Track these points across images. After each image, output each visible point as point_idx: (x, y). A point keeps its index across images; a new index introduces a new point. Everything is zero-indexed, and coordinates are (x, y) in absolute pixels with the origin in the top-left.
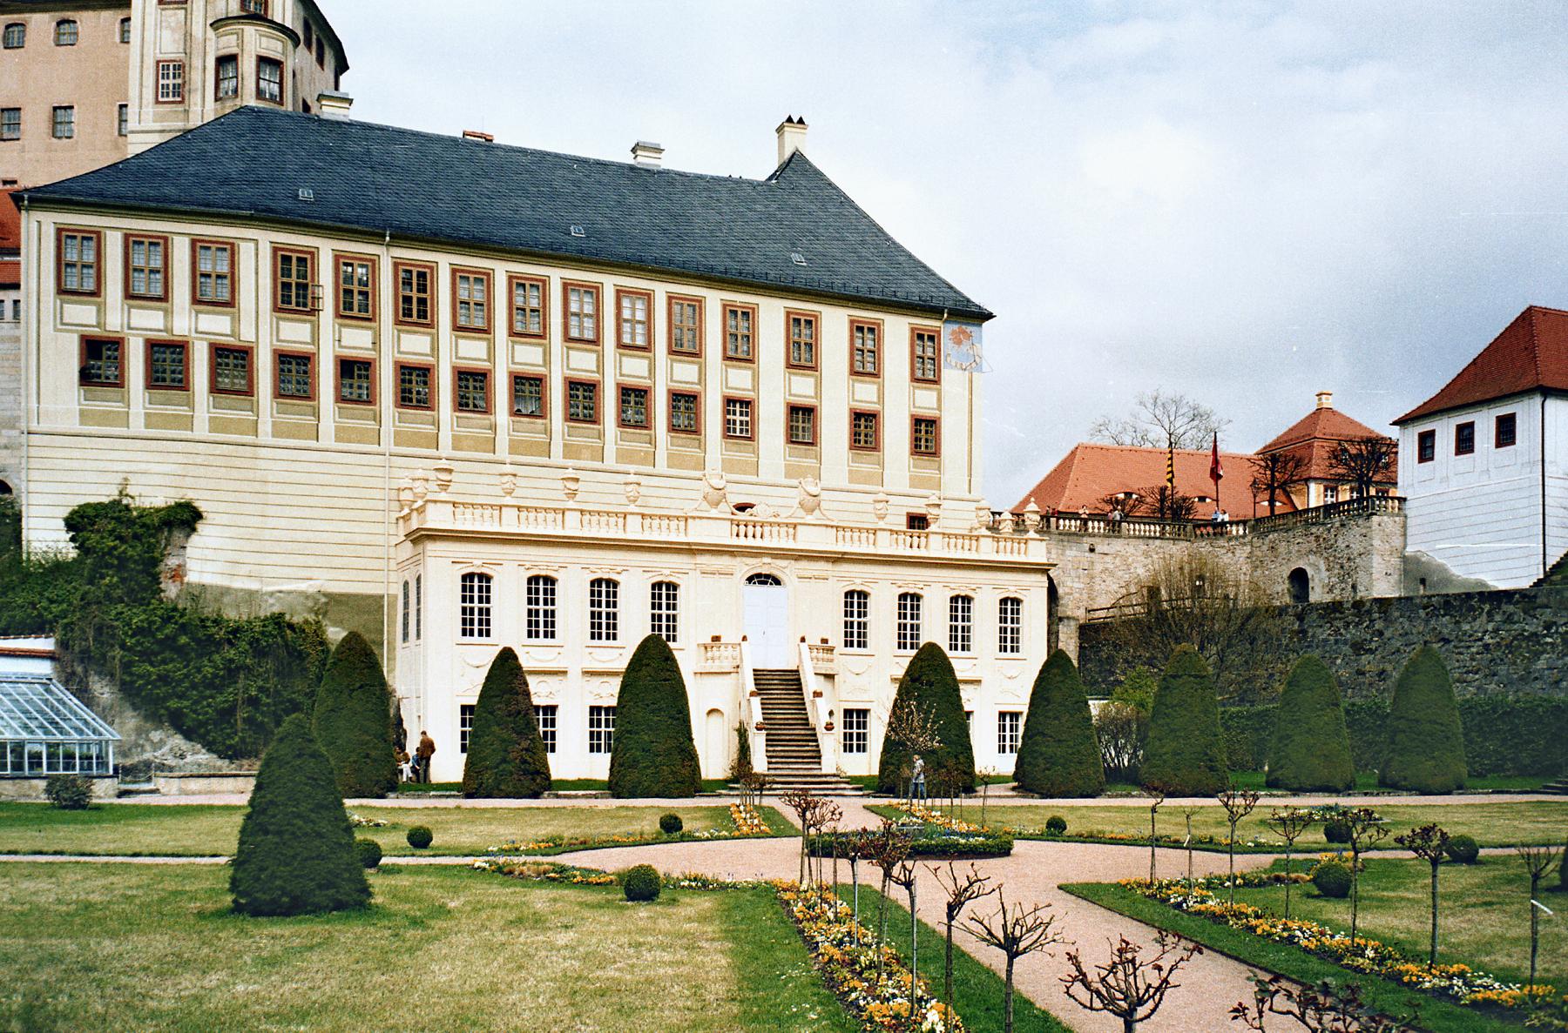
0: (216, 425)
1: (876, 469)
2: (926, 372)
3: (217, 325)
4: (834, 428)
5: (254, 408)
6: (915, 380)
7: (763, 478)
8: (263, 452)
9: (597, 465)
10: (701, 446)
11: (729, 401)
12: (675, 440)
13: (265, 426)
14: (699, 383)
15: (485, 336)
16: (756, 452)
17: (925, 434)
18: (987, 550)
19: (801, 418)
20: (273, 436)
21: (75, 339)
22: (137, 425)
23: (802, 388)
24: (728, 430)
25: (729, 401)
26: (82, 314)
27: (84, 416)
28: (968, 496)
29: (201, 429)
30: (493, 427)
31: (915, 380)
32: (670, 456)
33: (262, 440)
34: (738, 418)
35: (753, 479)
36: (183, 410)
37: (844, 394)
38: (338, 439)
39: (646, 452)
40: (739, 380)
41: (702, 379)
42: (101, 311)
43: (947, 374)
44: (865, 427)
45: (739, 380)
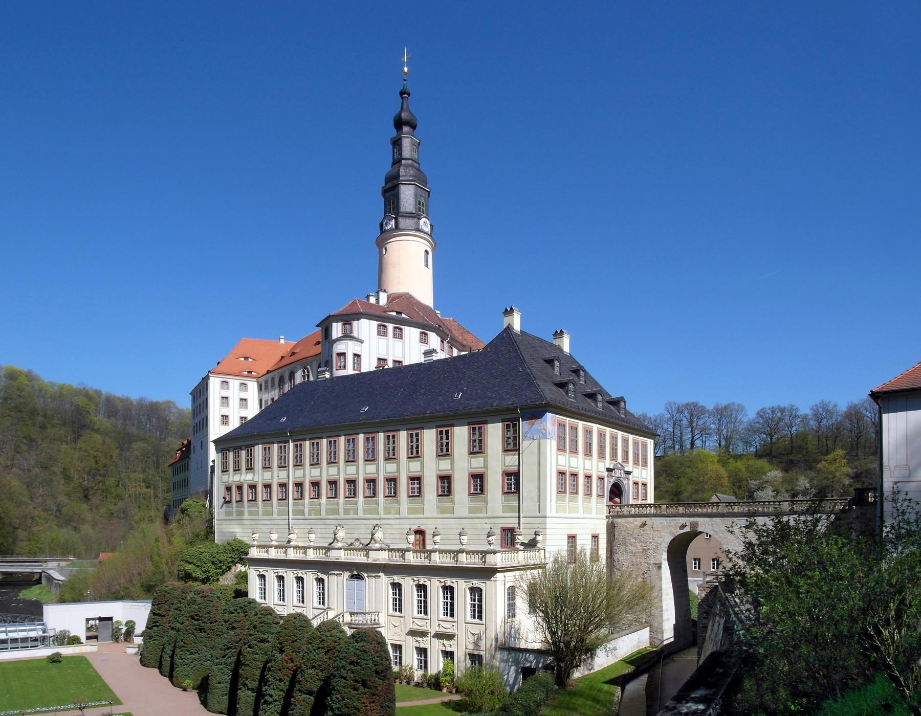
0: (250, 513)
2: (512, 445)
4: (461, 485)
5: (257, 506)
6: (505, 451)
7: (427, 515)
8: (261, 522)
9: (356, 516)
10: (399, 503)
11: (412, 479)
12: (387, 502)
13: (260, 513)
14: (397, 472)
16: (423, 502)
17: (513, 480)
19: (446, 481)
22: (235, 517)
26: (225, 478)
28: (538, 514)
29: (246, 516)
30: (320, 504)
31: (505, 451)
32: (385, 509)
35: (421, 516)
36: (242, 509)
37: (466, 465)
38: (278, 515)
39: (375, 509)
40: (415, 467)
41: (398, 471)
42: (229, 477)
43: (524, 444)
45: (415, 467)
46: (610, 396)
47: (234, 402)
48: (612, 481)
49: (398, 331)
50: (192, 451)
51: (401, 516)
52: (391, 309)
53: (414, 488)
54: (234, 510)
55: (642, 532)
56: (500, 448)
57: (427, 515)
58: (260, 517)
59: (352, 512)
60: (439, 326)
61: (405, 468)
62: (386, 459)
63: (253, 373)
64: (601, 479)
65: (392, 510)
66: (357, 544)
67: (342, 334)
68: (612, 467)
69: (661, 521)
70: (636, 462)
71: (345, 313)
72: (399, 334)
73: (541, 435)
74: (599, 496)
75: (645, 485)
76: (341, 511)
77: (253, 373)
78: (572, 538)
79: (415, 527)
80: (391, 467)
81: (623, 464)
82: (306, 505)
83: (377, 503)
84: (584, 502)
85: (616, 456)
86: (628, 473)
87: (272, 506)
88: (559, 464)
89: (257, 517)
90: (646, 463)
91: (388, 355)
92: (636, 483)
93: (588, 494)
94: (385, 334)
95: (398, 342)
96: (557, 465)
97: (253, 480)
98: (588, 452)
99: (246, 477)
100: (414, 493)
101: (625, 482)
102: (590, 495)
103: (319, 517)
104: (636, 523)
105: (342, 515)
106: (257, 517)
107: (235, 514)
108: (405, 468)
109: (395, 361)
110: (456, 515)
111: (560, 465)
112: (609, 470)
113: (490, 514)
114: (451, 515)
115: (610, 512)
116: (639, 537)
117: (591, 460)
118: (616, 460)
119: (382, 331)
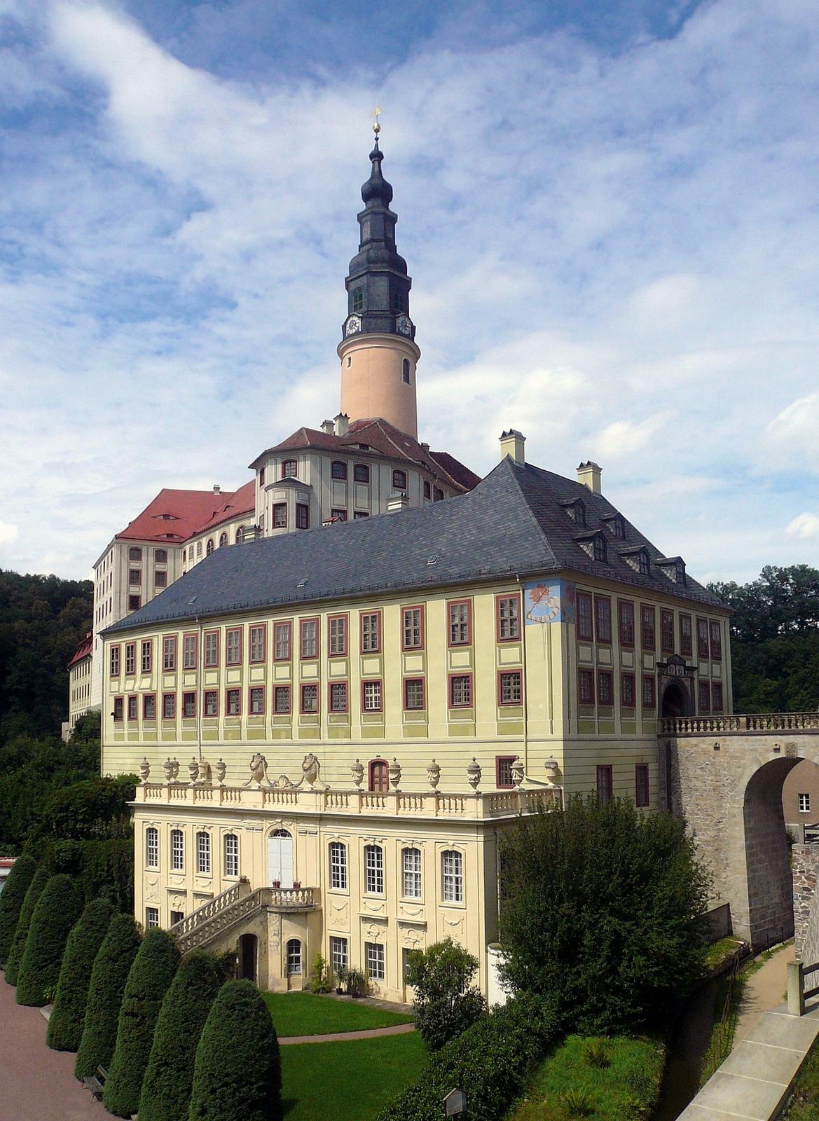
0: (146, 737)
1: (469, 721)
3: (146, 683)
4: (437, 693)
5: (156, 727)
7: (388, 738)
9: (289, 741)
10: (348, 720)
12: (332, 720)
13: (160, 736)
15: (192, 671)
18: (352, 807)
19: (414, 689)
20: (163, 740)
23: (414, 664)
24: (364, 709)
25: (366, 684)
28: (550, 736)
30: (240, 724)
34: (374, 695)
35: (381, 740)
37: (443, 663)
44: (461, 687)
45: (372, 666)
46: (664, 557)
47: (148, 577)
48: (665, 681)
49: (360, 470)
50: (94, 647)
51: (353, 740)
52: (354, 442)
53: (371, 698)
54: (126, 732)
55: (712, 760)
56: (493, 637)
57: (388, 738)
58: (160, 742)
59: (283, 734)
60: (423, 463)
61: (357, 669)
62: (330, 656)
63: (175, 536)
64: (648, 679)
65: (340, 731)
66: (282, 784)
68: (665, 662)
69: (741, 743)
70: (703, 655)
71: (288, 447)
72: (363, 475)
73: (552, 616)
74: (645, 705)
75: (718, 686)
76: (269, 734)
77: (175, 536)
78: (605, 772)
79: (373, 757)
80: (338, 668)
81: (683, 657)
82: (221, 725)
83: (318, 721)
84: (622, 715)
85: (672, 645)
86: (693, 669)
88: (581, 659)
89: (154, 743)
90: (720, 653)
91: (347, 505)
92: (704, 685)
93: (629, 703)
94: (344, 477)
95: (362, 488)
96: (578, 660)
97: (150, 688)
98: (627, 643)
100: (371, 706)
101: (687, 684)
102: (633, 704)
103: (239, 742)
104: (702, 746)
105: (270, 740)
106: (154, 743)
107: (126, 737)
110: (431, 739)
111: (582, 661)
112: (659, 665)
113: (479, 737)
114: (424, 739)
115: (663, 730)
116: (709, 767)
117: (631, 652)
118: (673, 652)
119: (339, 472)
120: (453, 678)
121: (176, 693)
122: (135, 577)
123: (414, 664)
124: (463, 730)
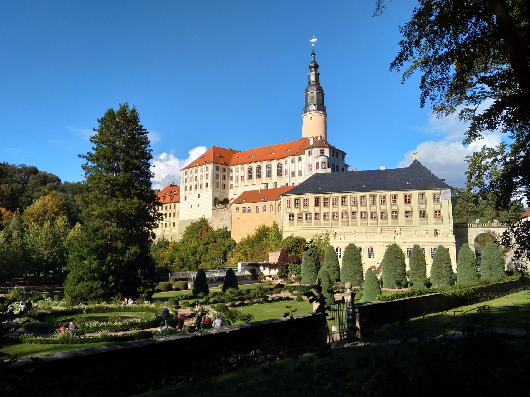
5: (312, 222)
13: (313, 225)
17: (437, 213)
21: (288, 214)
23: (408, 208)
26: (289, 211)
27: (290, 225)
28: (449, 225)
33: (313, 227)
40: (394, 208)
42: (291, 210)
44: (423, 214)
45: (394, 208)
47: (221, 177)
51: (389, 226)
61: (389, 207)
62: (380, 205)
67: (320, 153)
87: (320, 222)
95: (337, 159)
99: (304, 211)
108: (389, 207)
109: (336, 166)
113: (428, 225)
120: (371, 212)
121: (320, 213)
122: (217, 176)
123: (408, 208)
124: (424, 223)
